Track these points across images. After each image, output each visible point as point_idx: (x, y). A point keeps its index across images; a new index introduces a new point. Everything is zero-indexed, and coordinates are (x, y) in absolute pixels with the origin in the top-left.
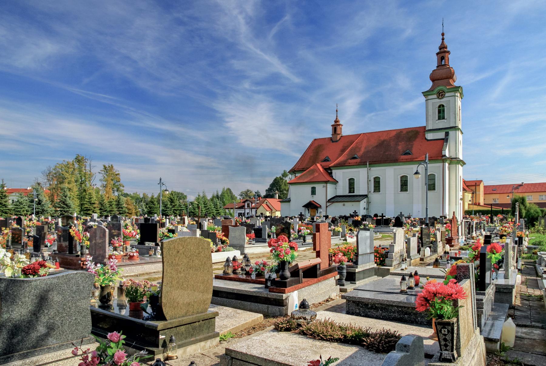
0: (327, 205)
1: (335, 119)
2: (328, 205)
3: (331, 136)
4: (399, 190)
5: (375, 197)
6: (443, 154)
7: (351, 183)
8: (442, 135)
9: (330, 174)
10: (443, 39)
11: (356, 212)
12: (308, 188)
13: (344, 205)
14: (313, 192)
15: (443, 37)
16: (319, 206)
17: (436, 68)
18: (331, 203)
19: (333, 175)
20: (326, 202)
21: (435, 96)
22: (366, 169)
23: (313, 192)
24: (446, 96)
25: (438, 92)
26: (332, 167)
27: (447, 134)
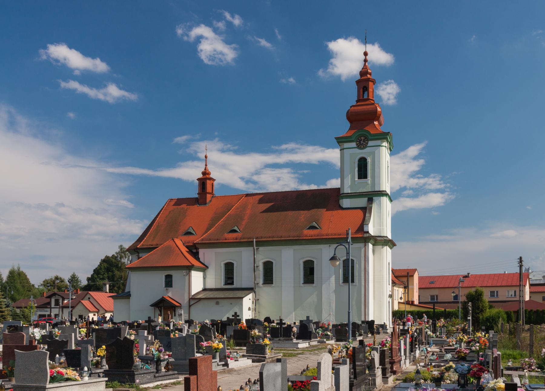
0: (190, 304)
1: (203, 170)
2: (192, 303)
3: (197, 196)
4: (302, 281)
5: (265, 292)
6: (365, 230)
8: (362, 202)
9: (196, 255)
12: (161, 277)
13: (217, 303)
14: (169, 282)
16: (177, 304)
17: (354, 103)
18: (198, 300)
19: (201, 256)
20: (190, 299)
21: (354, 145)
22: (252, 248)
23: (169, 282)
24: (368, 145)
26: (198, 244)
27: (370, 201)
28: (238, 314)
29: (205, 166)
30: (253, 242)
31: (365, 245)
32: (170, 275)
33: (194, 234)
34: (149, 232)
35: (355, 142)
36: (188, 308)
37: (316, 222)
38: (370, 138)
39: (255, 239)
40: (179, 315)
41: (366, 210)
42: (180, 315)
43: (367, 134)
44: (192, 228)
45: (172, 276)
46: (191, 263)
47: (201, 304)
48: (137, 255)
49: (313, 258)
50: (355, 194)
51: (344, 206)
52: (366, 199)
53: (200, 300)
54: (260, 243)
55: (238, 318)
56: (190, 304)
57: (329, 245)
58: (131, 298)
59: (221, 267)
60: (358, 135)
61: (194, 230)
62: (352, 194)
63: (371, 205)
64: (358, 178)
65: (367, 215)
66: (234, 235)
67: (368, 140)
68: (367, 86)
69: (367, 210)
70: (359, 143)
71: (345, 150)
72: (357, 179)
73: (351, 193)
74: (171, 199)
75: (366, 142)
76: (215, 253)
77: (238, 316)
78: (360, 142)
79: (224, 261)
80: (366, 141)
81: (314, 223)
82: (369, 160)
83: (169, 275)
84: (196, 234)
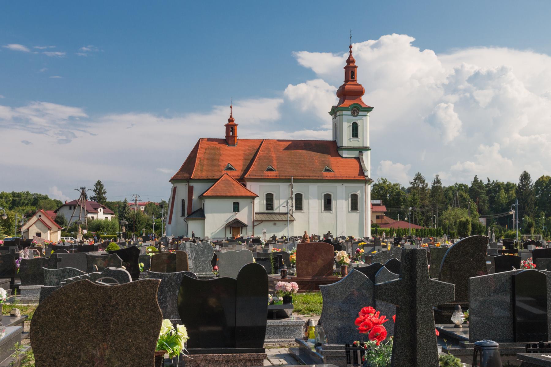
1: (229, 118)
3: (225, 138)
6: (366, 174)
7: (270, 199)
12: (229, 204)
13: (275, 224)
18: (260, 222)
19: (248, 187)
21: (349, 113)
22: (289, 184)
24: (359, 114)
30: (291, 179)
38: (361, 109)
41: (359, 159)
43: (358, 106)
47: (262, 225)
48: (187, 184)
49: (331, 192)
51: (344, 156)
54: (296, 181)
57: (342, 184)
58: (205, 219)
63: (362, 157)
64: (352, 137)
65: (362, 164)
66: (270, 173)
69: (361, 160)
72: (351, 137)
77: (331, 234)
79: (266, 192)
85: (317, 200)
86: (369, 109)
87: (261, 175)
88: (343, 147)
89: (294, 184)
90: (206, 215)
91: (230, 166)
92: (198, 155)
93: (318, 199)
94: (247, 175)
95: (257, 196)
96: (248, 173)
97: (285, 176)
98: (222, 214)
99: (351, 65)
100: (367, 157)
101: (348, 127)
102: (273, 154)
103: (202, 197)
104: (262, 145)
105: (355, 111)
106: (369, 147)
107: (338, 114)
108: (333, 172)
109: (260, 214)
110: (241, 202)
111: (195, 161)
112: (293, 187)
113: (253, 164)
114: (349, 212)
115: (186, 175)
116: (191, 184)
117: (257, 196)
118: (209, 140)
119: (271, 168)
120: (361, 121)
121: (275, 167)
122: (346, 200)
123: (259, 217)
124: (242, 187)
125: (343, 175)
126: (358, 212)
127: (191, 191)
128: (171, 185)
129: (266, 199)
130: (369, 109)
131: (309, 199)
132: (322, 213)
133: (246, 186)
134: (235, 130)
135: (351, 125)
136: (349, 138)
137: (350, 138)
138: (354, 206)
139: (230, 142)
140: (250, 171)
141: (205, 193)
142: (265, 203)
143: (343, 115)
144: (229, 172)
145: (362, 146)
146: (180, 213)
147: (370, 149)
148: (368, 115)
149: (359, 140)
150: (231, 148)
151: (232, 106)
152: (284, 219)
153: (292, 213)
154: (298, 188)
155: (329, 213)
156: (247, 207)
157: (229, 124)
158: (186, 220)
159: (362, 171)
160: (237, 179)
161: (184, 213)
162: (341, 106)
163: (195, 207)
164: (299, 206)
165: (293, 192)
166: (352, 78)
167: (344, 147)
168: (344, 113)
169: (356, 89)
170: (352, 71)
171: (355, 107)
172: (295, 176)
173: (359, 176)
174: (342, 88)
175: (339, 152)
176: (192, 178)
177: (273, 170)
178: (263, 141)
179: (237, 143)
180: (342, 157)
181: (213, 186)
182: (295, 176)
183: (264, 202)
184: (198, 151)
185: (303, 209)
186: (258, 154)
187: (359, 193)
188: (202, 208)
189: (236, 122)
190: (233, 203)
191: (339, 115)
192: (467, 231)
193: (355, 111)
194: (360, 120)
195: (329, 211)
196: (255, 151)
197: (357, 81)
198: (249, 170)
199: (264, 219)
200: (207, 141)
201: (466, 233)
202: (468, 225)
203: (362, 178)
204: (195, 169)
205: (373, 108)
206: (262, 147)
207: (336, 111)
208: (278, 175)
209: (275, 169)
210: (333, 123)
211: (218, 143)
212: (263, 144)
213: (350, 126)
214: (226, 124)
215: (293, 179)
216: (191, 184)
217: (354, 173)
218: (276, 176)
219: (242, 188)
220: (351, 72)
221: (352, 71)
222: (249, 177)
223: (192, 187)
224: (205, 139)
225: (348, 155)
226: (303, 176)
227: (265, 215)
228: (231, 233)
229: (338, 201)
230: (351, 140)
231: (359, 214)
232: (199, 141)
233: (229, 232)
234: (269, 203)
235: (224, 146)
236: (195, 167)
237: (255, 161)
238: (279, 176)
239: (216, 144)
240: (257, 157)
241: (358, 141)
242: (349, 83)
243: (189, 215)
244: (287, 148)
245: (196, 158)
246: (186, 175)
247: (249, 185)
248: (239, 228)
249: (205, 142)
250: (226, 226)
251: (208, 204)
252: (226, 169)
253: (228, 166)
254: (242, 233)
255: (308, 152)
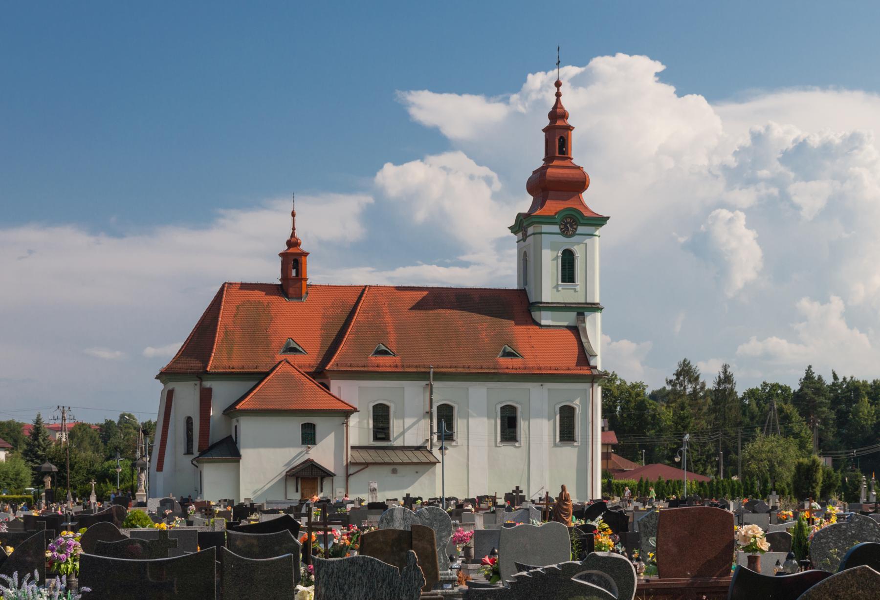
0: (349, 474)
1: (288, 238)
2: (351, 471)
3: (280, 283)
6: (592, 363)
10: (558, 95)
11: (515, 489)
12: (294, 426)
13: (394, 471)
15: (558, 90)
19: (334, 390)
21: (556, 228)
22: (424, 383)
24: (577, 232)
25: (564, 222)
28: (520, 489)
29: (292, 231)
30: (429, 373)
31: (592, 387)
32: (311, 424)
33: (301, 352)
34: (216, 344)
35: (558, 225)
36: (345, 478)
37: (509, 345)
38: (582, 221)
39: (432, 369)
40: (370, 490)
41: (577, 331)
42: (373, 490)
44: (291, 339)
45: (314, 425)
46: (353, 407)
47: (367, 473)
48: (198, 383)
49: (517, 402)
50: (558, 305)
51: (544, 322)
52: (574, 314)
53: (367, 467)
54: (441, 376)
55: (520, 494)
56: (349, 474)
57: (540, 383)
58: (241, 461)
59: (369, 411)
60: (567, 213)
61: (299, 345)
62: (555, 305)
63: (583, 325)
64: (562, 282)
65: (583, 340)
66: (382, 360)
67: (577, 225)
68: (566, 138)
69: (581, 332)
70: (565, 227)
71: (543, 235)
72: (560, 283)
73: (552, 303)
74: (228, 283)
75: (575, 227)
76: (359, 387)
77: (521, 492)
78: (566, 226)
80: (575, 225)
81: (506, 346)
82: (578, 255)
83: (308, 423)
84: (306, 352)
85: (485, 420)
86: (600, 221)
87: (362, 364)
88: (541, 303)
89: (436, 384)
90: (243, 452)
91: (293, 345)
92: (220, 319)
93: (489, 417)
94: (331, 363)
95: (355, 410)
96: (333, 360)
97: (416, 367)
98: (278, 450)
99: (559, 123)
100: (594, 324)
101: (553, 260)
102: (388, 319)
103: (231, 412)
104: (363, 298)
105: (568, 225)
106: (598, 304)
107: (530, 230)
108: (520, 358)
109: (359, 450)
110: (321, 424)
111: (215, 333)
112: (434, 390)
113: (345, 339)
114: (555, 445)
115: (195, 364)
116: (207, 384)
117: (355, 410)
118: (245, 286)
119: (384, 348)
120: (582, 246)
121: (393, 347)
122: (549, 420)
123: (361, 457)
124: (319, 389)
125: (542, 365)
126: (575, 444)
127: (206, 398)
128: (160, 386)
129: (374, 416)
130: (600, 221)
131: (467, 416)
132: (496, 446)
133: (328, 388)
134: (303, 265)
135: (560, 254)
136: (555, 284)
137: (558, 284)
138: (567, 434)
139: (291, 291)
140: (337, 355)
141: (241, 404)
142: (371, 426)
143: (541, 233)
144: (290, 357)
145: (583, 301)
146: (182, 448)
147: (601, 309)
148: (597, 233)
149: (578, 288)
150: (294, 303)
151: (296, 211)
152: (415, 460)
153: (431, 448)
154: (444, 392)
155: (512, 448)
156: (333, 435)
157: (288, 251)
158: (197, 463)
159: (584, 356)
160: (307, 373)
161: (192, 447)
162: (537, 213)
163: (217, 434)
164: (446, 434)
165: (433, 401)
166: (561, 152)
167: (544, 303)
168: (545, 228)
169: (571, 176)
170: (561, 138)
171: (571, 217)
172: (438, 367)
173: (579, 368)
174: (540, 173)
175: (533, 313)
176: (208, 369)
177: (390, 354)
178: (364, 290)
179: (307, 293)
180: (540, 325)
181: (258, 389)
182: (438, 367)
183: (368, 423)
184: (222, 311)
185: (455, 438)
186: (355, 317)
187: (576, 403)
188: (231, 436)
189: (303, 247)
190: (302, 425)
191: (534, 234)
192: (814, 485)
193: (568, 225)
194: (578, 244)
195: (512, 443)
196: (349, 310)
197: (572, 159)
198: (335, 353)
199: (369, 460)
200: (241, 288)
201: (810, 488)
202: (816, 472)
203: (585, 371)
204: (214, 351)
205: (608, 218)
206: (362, 302)
207: (525, 224)
208: (399, 364)
209: (394, 350)
210: (519, 250)
211: (264, 293)
212: (365, 295)
213: (557, 256)
214: (282, 251)
215: (434, 373)
216: (207, 384)
217: (568, 361)
218: (396, 367)
219: (321, 392)
220: (559, 140)
221: (561, 138)
222: (336, 368)
223: (210, 390)
224: (235, 284)
225: (553, 320)
226: (456, 367)
227: (372, 452)
228: (297, 491)
229: (531, 421)
230: (560, 288)
231: (577, 449)
232: (222, 290)
233: (294, 489)
234: (380, 425)
235: (276, 300)
236: (215, 347)
237: (348, 333)
238: (403, 367)
239: (259, 295)
240: (352, 324)
241: (575, 291)
242: (555, 163)
243: (204, 451)
244: (420, 306)
245: (216, 325)
246: (195, 364)
247: (335, 386)
248: (316, 478)
249: (235, 291)
250: (286, 475)
251: (247, 428)
252: (283, 352)
253: (289, 343)
254: (322, 491)
255: (465, 313)
